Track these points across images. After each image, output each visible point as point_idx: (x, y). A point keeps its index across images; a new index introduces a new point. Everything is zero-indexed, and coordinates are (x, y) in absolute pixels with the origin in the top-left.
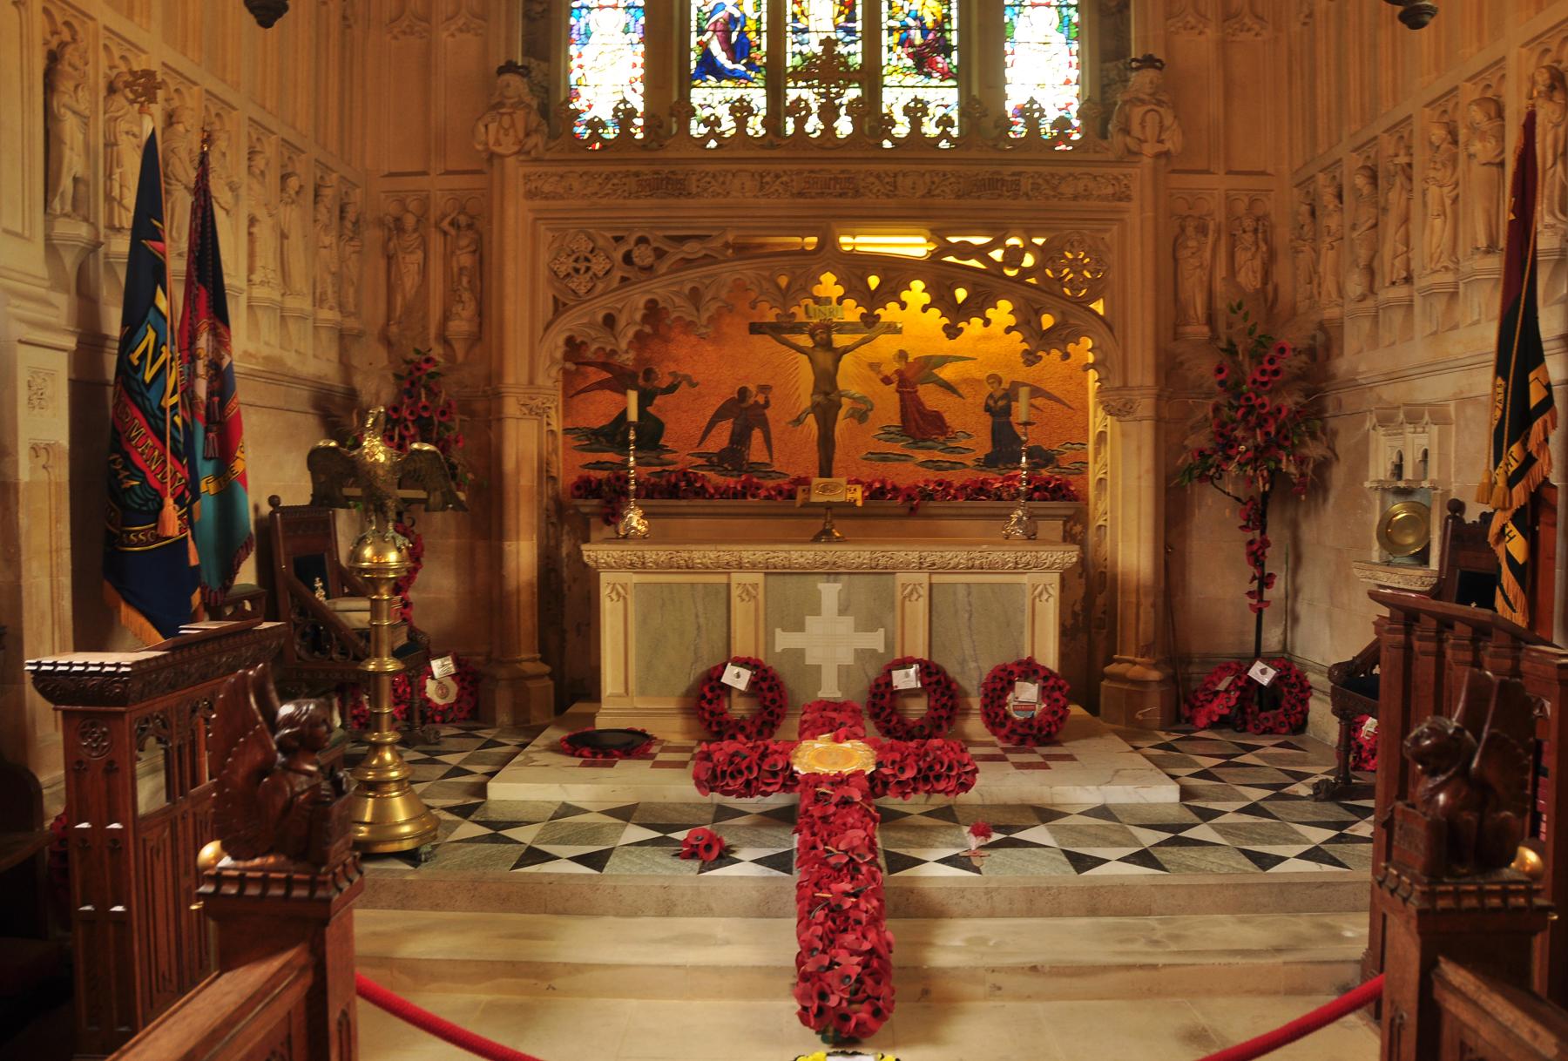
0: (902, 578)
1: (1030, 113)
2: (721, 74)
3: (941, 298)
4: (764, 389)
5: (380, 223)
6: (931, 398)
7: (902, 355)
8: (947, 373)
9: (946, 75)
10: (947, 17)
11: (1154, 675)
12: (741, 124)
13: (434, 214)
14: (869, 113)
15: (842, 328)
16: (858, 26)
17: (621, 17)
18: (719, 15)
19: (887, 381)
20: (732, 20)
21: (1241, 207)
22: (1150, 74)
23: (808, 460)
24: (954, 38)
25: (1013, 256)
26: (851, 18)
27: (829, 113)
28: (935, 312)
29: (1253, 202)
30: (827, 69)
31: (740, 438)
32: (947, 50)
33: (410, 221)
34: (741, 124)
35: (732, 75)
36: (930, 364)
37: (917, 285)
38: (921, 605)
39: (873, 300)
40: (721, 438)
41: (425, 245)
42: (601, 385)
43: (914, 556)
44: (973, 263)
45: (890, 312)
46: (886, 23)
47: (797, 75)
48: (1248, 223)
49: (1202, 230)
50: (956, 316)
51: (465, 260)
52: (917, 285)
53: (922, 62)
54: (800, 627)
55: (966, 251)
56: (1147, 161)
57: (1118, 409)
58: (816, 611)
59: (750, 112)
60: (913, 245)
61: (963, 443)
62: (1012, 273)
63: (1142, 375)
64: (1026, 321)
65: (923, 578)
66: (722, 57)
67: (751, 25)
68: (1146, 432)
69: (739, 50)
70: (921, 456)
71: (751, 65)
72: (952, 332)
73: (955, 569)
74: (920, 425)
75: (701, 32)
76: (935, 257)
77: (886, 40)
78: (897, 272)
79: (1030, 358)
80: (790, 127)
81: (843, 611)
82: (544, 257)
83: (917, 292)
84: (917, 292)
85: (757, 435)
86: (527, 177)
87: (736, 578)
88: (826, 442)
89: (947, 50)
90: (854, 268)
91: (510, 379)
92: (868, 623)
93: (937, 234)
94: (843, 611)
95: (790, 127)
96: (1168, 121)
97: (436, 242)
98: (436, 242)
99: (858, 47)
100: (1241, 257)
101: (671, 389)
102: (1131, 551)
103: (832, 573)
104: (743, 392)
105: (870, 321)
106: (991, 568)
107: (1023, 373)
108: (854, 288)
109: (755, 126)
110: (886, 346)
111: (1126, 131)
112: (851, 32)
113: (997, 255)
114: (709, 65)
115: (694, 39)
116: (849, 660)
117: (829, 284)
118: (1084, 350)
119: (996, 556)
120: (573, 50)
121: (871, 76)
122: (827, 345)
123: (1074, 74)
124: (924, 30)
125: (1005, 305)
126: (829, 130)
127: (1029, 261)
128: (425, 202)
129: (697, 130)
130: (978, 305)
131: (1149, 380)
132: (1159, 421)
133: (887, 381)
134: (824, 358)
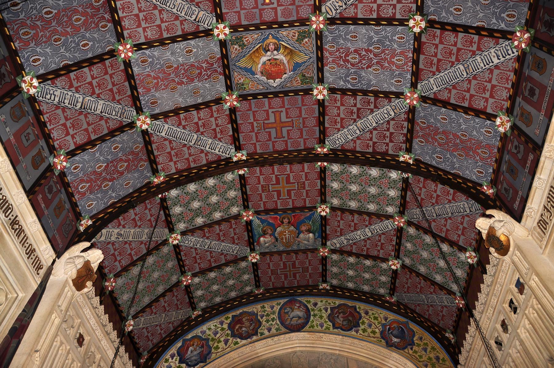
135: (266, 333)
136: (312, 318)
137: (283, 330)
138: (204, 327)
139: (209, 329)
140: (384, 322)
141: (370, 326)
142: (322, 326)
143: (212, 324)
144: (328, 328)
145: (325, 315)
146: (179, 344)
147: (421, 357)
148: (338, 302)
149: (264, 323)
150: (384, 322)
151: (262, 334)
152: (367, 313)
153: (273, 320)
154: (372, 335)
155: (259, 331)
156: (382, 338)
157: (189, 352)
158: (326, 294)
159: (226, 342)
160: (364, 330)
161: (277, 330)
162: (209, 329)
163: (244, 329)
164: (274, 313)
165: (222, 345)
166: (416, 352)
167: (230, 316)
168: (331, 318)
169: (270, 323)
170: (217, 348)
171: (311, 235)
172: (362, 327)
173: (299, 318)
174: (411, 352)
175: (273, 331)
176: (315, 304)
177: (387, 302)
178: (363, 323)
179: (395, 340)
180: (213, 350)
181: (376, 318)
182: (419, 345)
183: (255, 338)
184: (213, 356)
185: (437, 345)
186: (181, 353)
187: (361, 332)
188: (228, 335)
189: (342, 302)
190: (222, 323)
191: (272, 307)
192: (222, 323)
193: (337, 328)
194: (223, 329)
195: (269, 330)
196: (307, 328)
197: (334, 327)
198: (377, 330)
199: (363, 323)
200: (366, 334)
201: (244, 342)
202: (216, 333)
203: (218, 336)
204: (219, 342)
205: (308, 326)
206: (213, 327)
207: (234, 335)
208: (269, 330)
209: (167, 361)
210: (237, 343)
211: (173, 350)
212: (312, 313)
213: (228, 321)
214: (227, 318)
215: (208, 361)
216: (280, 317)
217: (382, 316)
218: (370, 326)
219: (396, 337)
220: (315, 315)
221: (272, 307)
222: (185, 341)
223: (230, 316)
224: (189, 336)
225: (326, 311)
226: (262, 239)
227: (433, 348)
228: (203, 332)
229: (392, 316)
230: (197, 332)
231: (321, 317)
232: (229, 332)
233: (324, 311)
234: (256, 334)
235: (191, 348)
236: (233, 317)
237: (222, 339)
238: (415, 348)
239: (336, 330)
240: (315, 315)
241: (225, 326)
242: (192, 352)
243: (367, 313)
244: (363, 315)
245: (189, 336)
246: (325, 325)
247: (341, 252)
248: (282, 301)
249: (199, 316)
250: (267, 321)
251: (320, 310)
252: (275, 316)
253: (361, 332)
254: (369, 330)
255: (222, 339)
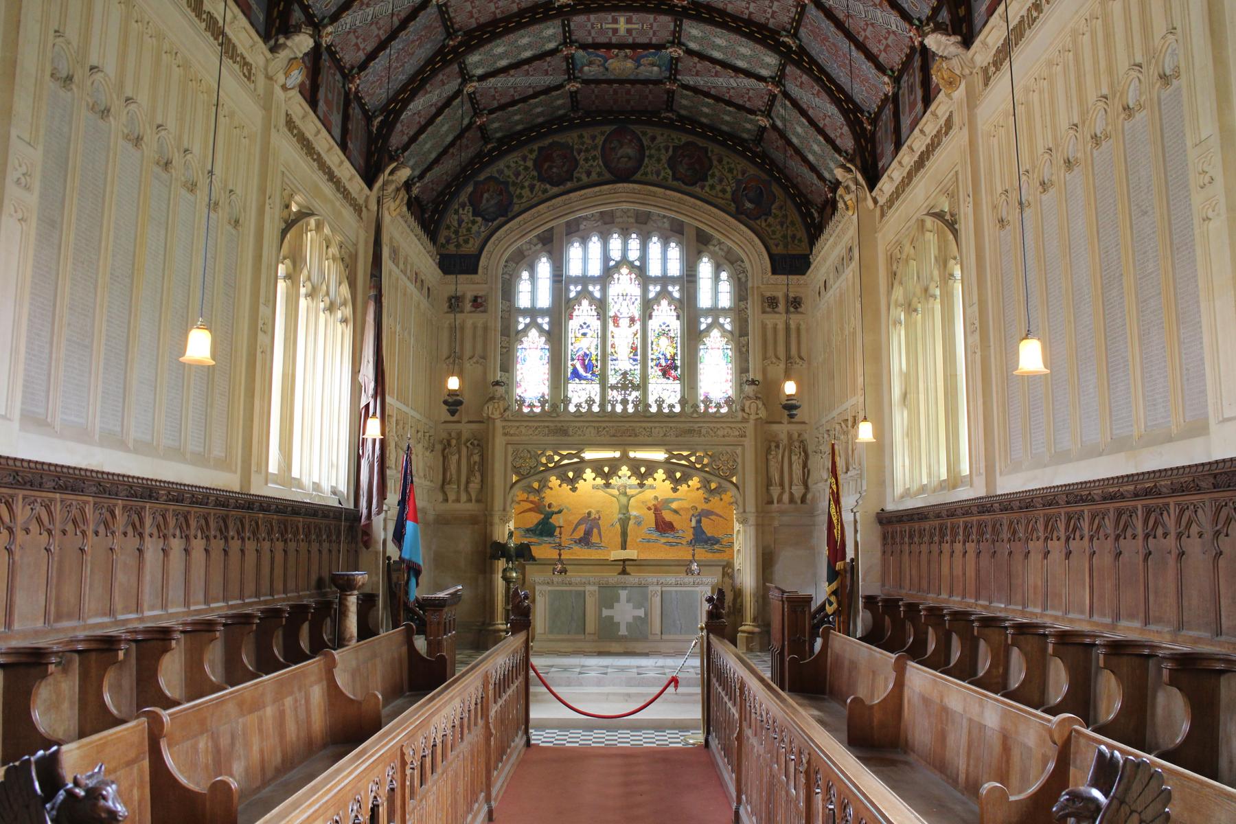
0: (650, 588)
1: (707, 401)
2: (580, 377)
3: (670, 476)
4: (598, 512)
5: (441, 442)
6: (668, 516)
7: (656, 498)
8: (674, 506)
9: (675, 378)
10: (676, 354)
11: (757, 630)
12: (590, 406)
13: (463, 439)
14: (643, 402)
15: (631, 487)
16: (638, 358)
17: (539, 353)
18: (581, 353)
19: (649, 509)
20: (586, 355)
21: (796, 436)
22: (753, 387)
23: (619, 540)
24: (678, 363)
25: (699, 460)
26: (635, 355)
27: (625, 402)
28: (667, 482)
29: (799, 435)
30: (625, 384)
31: (588, 533)
32: (675, 368)
33: (454, 442)
34: (590, 406)
35: (585, 379)
36: (667, 502)
37: (661, 471)
38: (657, 601)
39: (642, 477)
40: (580, 533)
41: (459, 452)
42: (530, 510)
43: (655, 580)
44: (683, 462)
45: (650, 481)
46: (650, 357)
47: (613, 387)
48: (797, 444)
49: (777, 447)
50: (676, 482)
51: (476, 458)
52: (661, 471)
53: (665, 373)
54: (612, 607)
55: (680, 457)
56: (752, 422)
57: (744, 521)
58: (618, 600)
59: (594, 402)
60: (659, 455)
61: (681, 534)
62: (698, 466)
63: (751, 508)
64: (705, 484)
65: (659, 588)
66: (581, 371)
67: (594, 357)
68: (751, 531)
69: (588, 367)
70: (663, 540)
71: (593, 374)
72: (675, 490)
73: (671, 585)
74: (663, 527)
75: (573, 359)
76: (667, 461)
77: (651, 364)
78: (652, 466)
79: (707, 500)
80: (609, 408)
81: (628, 601)
82: (510, 459)
83: (660, 474)
84: (660, 474)
85: (595, 531)
86: (504, 427)
87: (588, 588)
88: (624, 534)
89: (675, 368)
90: (635, 465)
91: (496, 508)
92: (638, 606)
93: (668, 451)
94: (628, 601)
95: (609, 408)
96: (760, 405)
97: (464, 451)
98: (464, 451)
99: (638, 367)
100: (794, 458)
101: (560, 512)
102: (747, 578)
103: (624, 588)
104: (589, 514)
105: (641, 485)
106: (684, 585)
107: (705, 506)
108: (635, 471)
109: (596, 409)
110: (649, 495)
111: (743, 410)
112: (635, 360)
113: (693, 459)
114: (576, 374)
115: (570, 363)
116: (631, 620)
117: (624, 470)
118: (727, 497)
119: (686, 580)
120: (519, 366)
121: (643, 386)
122: (625, 494)
123: (730, 377)
124: (666, 359)
125: (696, 479)
126: (625, 409)
127: (706, 461)
128: (459, 435)
129: (572, 409)
130: (685, 478)
131: (753, 510)
132: (757, 525)
133: (649, 509)
134: (624, 500)
135: (585, 178)
136: (646, 160)
137: (607, 176)
138: (501, 164)
139: (508, 167)
140: (740, 177)
141: (721, 181)
142: (658, 174)
143: (512, 159)
144: (665, 179)
145: (664, 158)
146: (470, 189)
147: (774, 232)
148: (685, 138)
149: (582, 162)
150: (740, 177)
151: (579, 179)
152: (720, 161)
153: (594, 158)
154: (720, 195)
155: (575, 175)
156: (733, 200)
157: (484, 201)
158: (670, 125)
159: (532, 188)
160: (712, 187)
161: (599, 174)
162: (508, 167)
163: (555, 170)
164: (595, 148)
165: (526, 192)
166: (769, 225)
167: (536, 147)
168: (672, 163)
169: (591, 162)
170: (520, 196)
171: (655, 68)
172: (710, 182)
173: (630, 158)
174: (764, 225)
175: (594, 176)
176: (653, 139)
177: (750, 150)
178: (713, 176)
179: (749, 205)
180: (515, 200)
181: (731, 170)
182: (776, 217)
183: (569, 185)
184: (516, 208)
185: (798, 219)
186: (474, 201)
187: (707, 189)
188: (533, 178)
189: (691, 138)
190: (524, 158)
191: (594, 138)
192: (524, 158)
193: (677, 179)
194: (526, 168)
195: (589, 174)
196: (638, 176)
197: (675, 178)
198: (728, 189)
199: (713, 176)
200: (713, 193)
201: (555, 190)
202: (517, 174)
203: (521, 178)
204: (523, 187)
205: (640, 173)
206: (513, 165)
207: (541, 179)
208: (589, 174)
209: (456, 212)
210: (545, 191)
211: (463, 197)
212: (647, 153)
213: (533, 156)
214: (531, 151)
215: (510, 215)
216: (603, 156)
217: (739, 167)
218: (721, 181)
219: (750, 201)
220: (651, 157)
221: (594, 138)
222: (476, 184)
223: (536, 147)
224: (482, 177)
225: (667, 150)
226: (586, 69)
227: (793, 223)
228: (501, 172)
229: (752, 170)
230: (492, 171)
231: (659, 160)
232: (535, 174)
233: (663, 151)
234: (571, 179)
235: (486, 195)
236: (540, 149)
237: (526, 184)
238: (770, 220)
239: (675, 183)
240: (651, 157)
241: (530, 164)
242: (488, 201)
243: (720, 161)
244: (715, 163)
245: (482, 177)
246: (663, 174)
247: (695, 90)
248: (608, 129)
249: (493, 149)
250: (586, 160)
251: (659, 149)
252: (597, 153)
253: (707, 189)
254: (718, 188)
255: (526, 184)
